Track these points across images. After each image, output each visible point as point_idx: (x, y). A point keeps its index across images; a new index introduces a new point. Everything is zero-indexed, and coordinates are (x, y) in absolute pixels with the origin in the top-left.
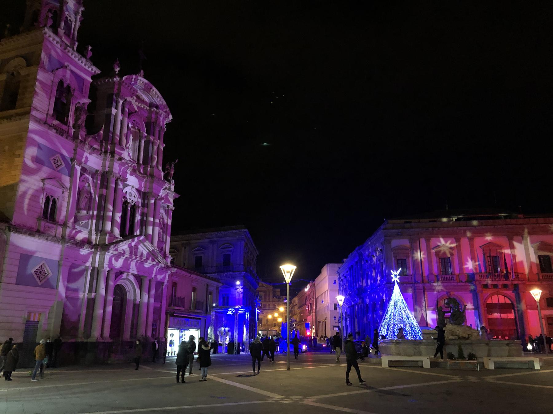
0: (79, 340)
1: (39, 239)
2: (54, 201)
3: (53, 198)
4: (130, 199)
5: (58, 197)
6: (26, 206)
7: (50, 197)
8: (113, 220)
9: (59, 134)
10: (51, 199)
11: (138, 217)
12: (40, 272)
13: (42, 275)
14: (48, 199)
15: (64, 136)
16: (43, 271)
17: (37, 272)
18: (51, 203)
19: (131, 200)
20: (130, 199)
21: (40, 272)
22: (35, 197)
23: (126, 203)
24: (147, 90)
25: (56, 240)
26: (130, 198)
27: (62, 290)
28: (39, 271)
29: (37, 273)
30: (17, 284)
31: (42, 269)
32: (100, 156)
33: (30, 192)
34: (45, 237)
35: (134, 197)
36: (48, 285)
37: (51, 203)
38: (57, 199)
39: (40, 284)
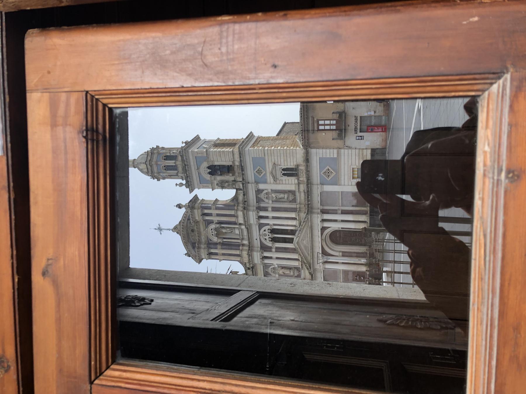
0: (369, 208)
20: (269, 235)
35: (265, 231)
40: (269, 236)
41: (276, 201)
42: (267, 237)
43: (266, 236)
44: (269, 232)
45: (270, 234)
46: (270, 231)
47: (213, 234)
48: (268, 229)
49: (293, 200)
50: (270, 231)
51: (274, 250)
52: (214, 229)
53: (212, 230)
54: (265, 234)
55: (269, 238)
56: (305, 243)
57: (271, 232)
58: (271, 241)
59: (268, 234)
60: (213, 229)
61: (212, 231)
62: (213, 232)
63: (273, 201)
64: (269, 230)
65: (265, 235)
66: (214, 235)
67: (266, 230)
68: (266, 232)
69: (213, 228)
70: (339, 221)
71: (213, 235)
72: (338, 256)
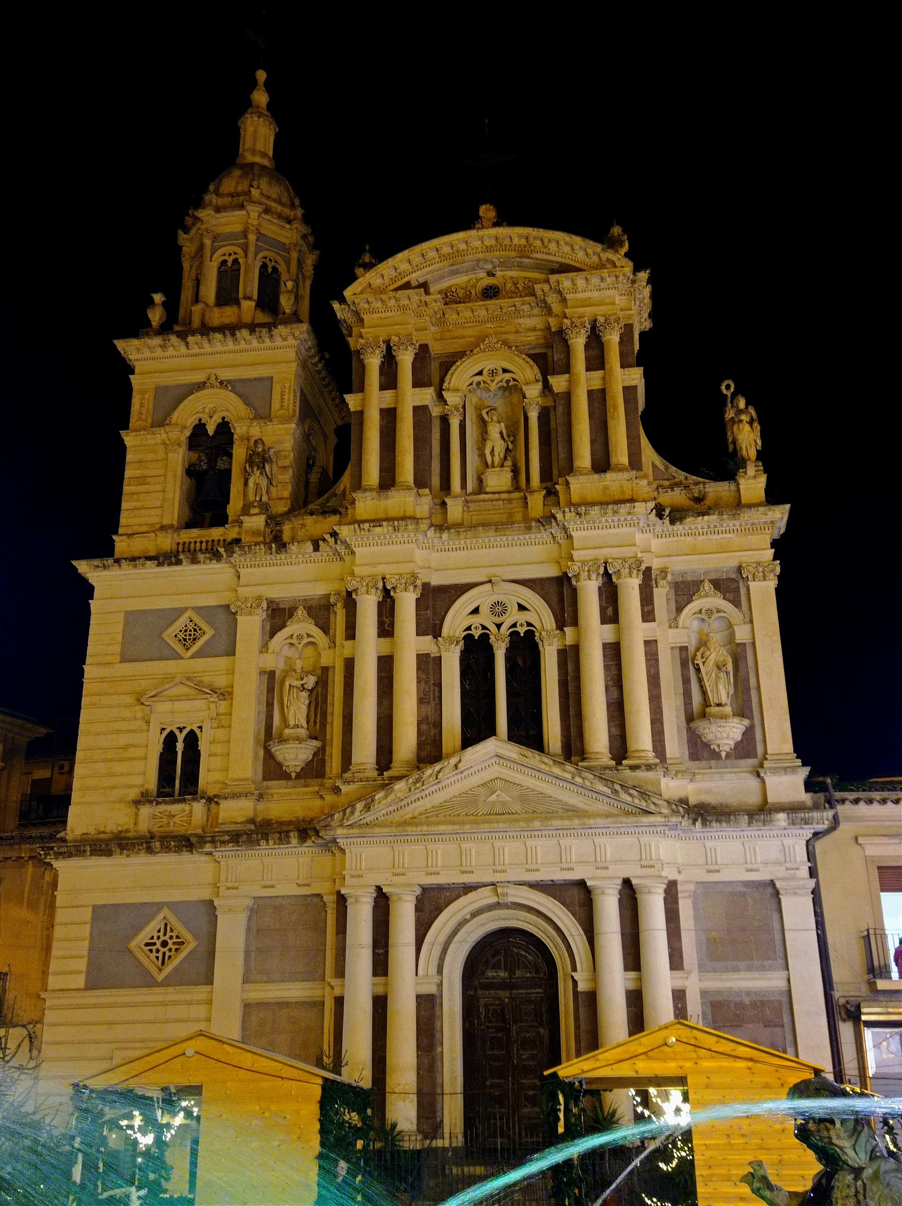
1: (128, 856)
3: (185, 732)
4: (499, 626)
5: (199, 725)
7: (177, 732)
9: (170, 564)
10: (181, 737)
12: (164, 944)
13: (158, 951)
18: (180, 746)
19: (504, 628)
20: (499, 626)
25: (175, 846)
26: (498, 620)
28: (158, 943)
29: (154, 948)
32: (318, 554)
34: (141, 847)
35: (521, 608)
37: (180, 746)
38: (198, 731)
40: (493, 629)
41: (684, 664)
42: (486, 619)
43: (493, 613)
44: (514, 625)
46: (522, 630)
47: (485, 377)
48: (529, 624)
49: (707, 745)
50: (522, 630)
51: (427, 644)
52: (508, 382)
53: (505, 371)
54: (504, 612)
55: (484, 627)
56: (493, 798)
57: (514, 635)
58: (468, 638)
60: (507, 376)
62: (498, 379)
63: (683, 649)
64: (525, 628)
65: (499, 609)
66: (479, 378)
67: (526, 612)
68: (513, 616)
69: (519, 375)
70: (640, 980)
71: (480, 373)
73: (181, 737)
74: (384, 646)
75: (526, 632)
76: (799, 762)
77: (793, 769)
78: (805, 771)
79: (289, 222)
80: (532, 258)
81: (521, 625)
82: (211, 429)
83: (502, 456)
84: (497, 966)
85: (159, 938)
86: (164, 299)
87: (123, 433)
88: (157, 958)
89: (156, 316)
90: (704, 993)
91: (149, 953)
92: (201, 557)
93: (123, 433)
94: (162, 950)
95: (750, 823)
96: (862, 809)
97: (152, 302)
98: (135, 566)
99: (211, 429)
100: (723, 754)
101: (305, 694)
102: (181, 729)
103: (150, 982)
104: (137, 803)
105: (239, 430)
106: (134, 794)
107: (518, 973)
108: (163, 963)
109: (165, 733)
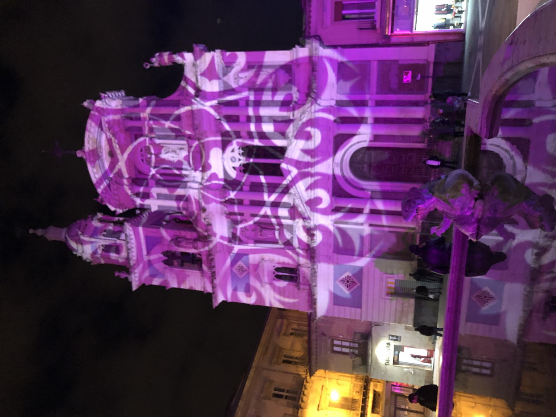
2: (277, 269)
3: (275, 272)
4: (240, 160)
6: (291, 301)
7: (275, 274)
8: (275, 205)
9: (215, 275)
10: (277, 273)
11: (257, 142)
14: (279, 278)
15: (214, 270)
16: (346, 279)
17: (348, 285)
18: (280, 274)
20: (240, 160)
21: (348, 282)
22: (281, 292)
23: (245, 169)
24: (95, 154)
26: (237, 160)
27: (362, 262)
29: (349, 285)
30: (360, 307)
31: (344, 280)
33: (278, 297)
35: (233, 151)
36: (359, 274)
38: (275, 268)
39: (358, 285)
44: (240, 154)
45: (242, 158)
53: (141, 151)
59: (237, 156)
60: (143, 150)
61: (142, 153)
65: (233, 159)
71: (143, 160)
72: (363, 198)
73: (277, 273)
74: (246, 202)
75: (242, 149)
76: (294, 49)
77: (297, 51)
78: (297, 46)
79: (86, 225)
80: (97, 137)
81: (240, 151)
82: (166, 258)
83: (174, 153)
84: (363, 168)
85: (346, 283)
86: (117, 272)
87: (167, 289)
88: (352, 284)
89: (123, 275)
90: (377, 93)
91: (350, 287)
92: (213, 265)
93: (167, 289)
94: (350, 282)
95: (316, 71)
96: (312, 25)
97: (118, 276)
98: (216, 287)
99: (166, 258)
100: (290, 78)
101: (263, 231)
102: (274, 273)
103: (361, 287)
104: (299, 289)
105: (166, 249)
106: (296, 290)
107: (366, 160)
108: (354, 282)
109: (275, 278)
